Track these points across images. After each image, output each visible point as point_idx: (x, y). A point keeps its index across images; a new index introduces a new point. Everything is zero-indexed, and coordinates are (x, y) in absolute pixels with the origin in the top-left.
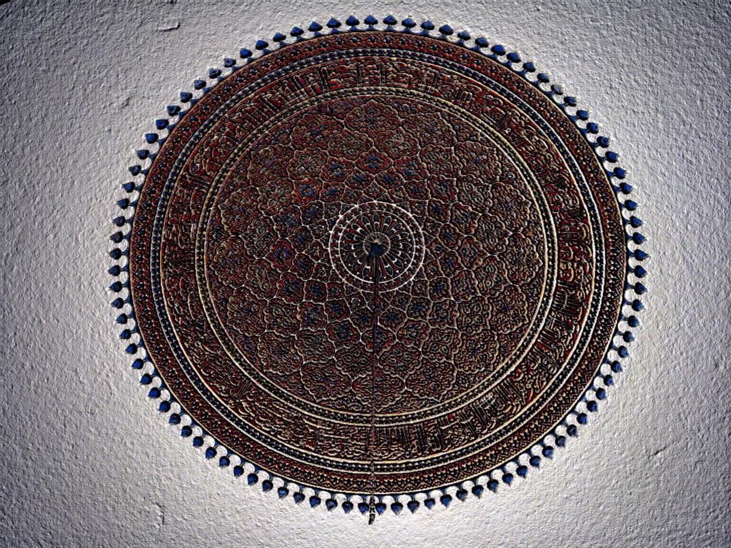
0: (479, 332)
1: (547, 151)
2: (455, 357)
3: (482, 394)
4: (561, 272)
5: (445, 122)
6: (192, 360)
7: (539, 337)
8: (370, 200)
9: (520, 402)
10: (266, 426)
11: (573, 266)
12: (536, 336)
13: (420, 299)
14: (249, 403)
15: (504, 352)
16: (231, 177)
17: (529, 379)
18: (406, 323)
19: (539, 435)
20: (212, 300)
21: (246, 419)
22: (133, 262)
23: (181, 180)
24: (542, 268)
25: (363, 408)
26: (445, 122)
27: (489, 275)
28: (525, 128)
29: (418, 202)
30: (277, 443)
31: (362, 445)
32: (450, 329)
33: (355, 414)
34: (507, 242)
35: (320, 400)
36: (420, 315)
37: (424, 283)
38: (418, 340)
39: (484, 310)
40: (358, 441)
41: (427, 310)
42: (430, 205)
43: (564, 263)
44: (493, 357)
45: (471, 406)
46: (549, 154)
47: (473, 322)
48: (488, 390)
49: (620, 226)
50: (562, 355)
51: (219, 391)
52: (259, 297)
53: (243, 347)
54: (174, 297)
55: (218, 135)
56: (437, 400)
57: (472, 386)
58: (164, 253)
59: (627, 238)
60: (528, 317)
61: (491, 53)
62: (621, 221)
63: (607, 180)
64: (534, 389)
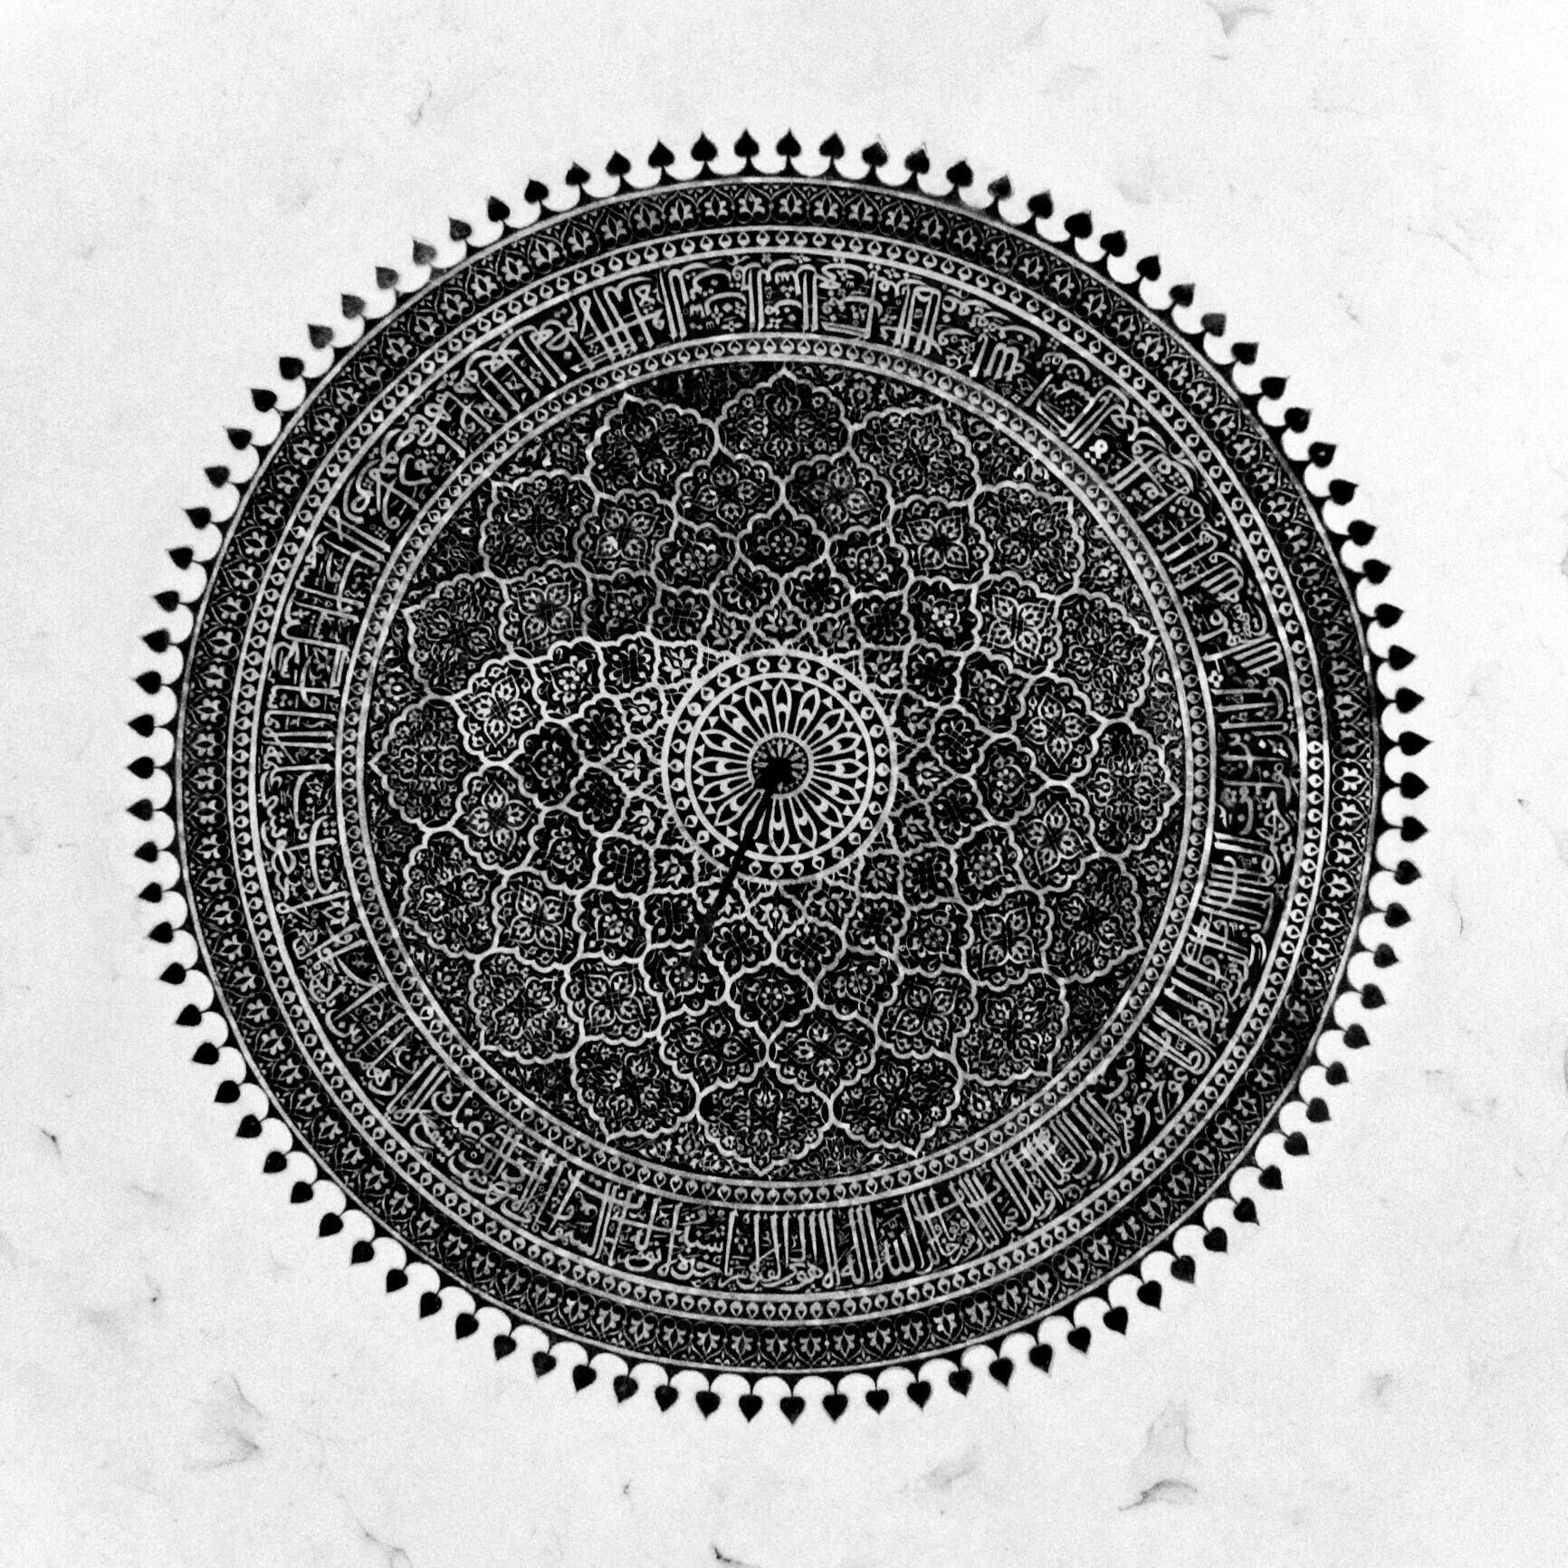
0: (1022, 980)
1: (1190, 495)
2: (959, 1045)
3: (1021, 1135)
4: (1223, 814)
5: (954, 431)
6: (308, 994)
7: (1168, 984)
8: (767, 645)
9: (1118, 1149)
10: (474, 1182)
11: (1252, 790)
12: (1163, 978)
13: (879, 902)
14: (439, 1120)
15: (1085, 1027)
16: (439, 541)
17: (1141, 1091)
18: (842, 963)
19: (1162, 1229)
20: (366, 846)
21: (428, 1159)
22: (188, 715)
23: (321, 528)
24: (1180, 806)
25: (724, 1164)
26: (954, 431)
27: (1053, 838)
28: (1142, 436)
29: (886, 654)
30: (501, 1227)
31: (715, 1253)
32: (950, 976)
33: (702, 1178)
34: (1096, 746)
35: (614, 1136)
36: (879, 941)
37: (891, 862)
38: (870, 1003)
39: (1035, 925)
40: (704, 1243)
41: (896, 929)
42: (912, 659)
43: (1233, 788)
44: (1054, 1041)
45: (994, 1164)
46: (1196, 503)
47: (1008, 957)
48: (1037, 1124)
49: (1364, 675)
50: (1223, 1025)
51: (367, 1080)
52: (485, 860)
53: (435, 980)
54: (277, 822)
55: (420, 423)
56: (908, 1151)
57: (1000, 1116)
58: (264, 709)
59: (1382, 702)
60: (1144, 936)
61: (1063, 236)
62: (1366, 661)
63: (1333, 557)
64: (1152, 1114)
